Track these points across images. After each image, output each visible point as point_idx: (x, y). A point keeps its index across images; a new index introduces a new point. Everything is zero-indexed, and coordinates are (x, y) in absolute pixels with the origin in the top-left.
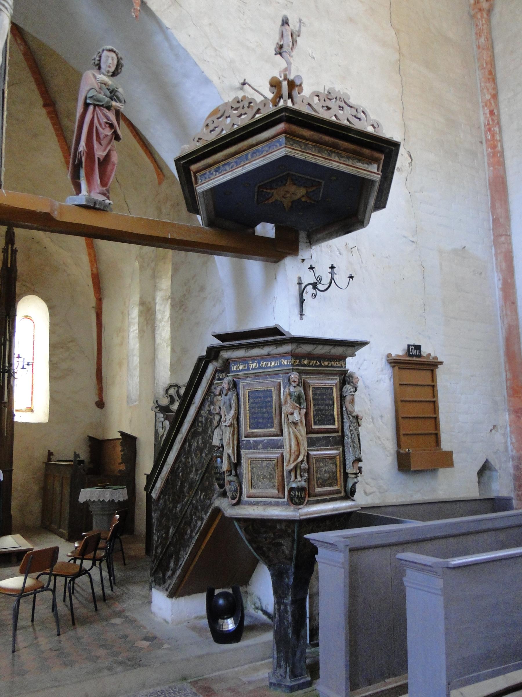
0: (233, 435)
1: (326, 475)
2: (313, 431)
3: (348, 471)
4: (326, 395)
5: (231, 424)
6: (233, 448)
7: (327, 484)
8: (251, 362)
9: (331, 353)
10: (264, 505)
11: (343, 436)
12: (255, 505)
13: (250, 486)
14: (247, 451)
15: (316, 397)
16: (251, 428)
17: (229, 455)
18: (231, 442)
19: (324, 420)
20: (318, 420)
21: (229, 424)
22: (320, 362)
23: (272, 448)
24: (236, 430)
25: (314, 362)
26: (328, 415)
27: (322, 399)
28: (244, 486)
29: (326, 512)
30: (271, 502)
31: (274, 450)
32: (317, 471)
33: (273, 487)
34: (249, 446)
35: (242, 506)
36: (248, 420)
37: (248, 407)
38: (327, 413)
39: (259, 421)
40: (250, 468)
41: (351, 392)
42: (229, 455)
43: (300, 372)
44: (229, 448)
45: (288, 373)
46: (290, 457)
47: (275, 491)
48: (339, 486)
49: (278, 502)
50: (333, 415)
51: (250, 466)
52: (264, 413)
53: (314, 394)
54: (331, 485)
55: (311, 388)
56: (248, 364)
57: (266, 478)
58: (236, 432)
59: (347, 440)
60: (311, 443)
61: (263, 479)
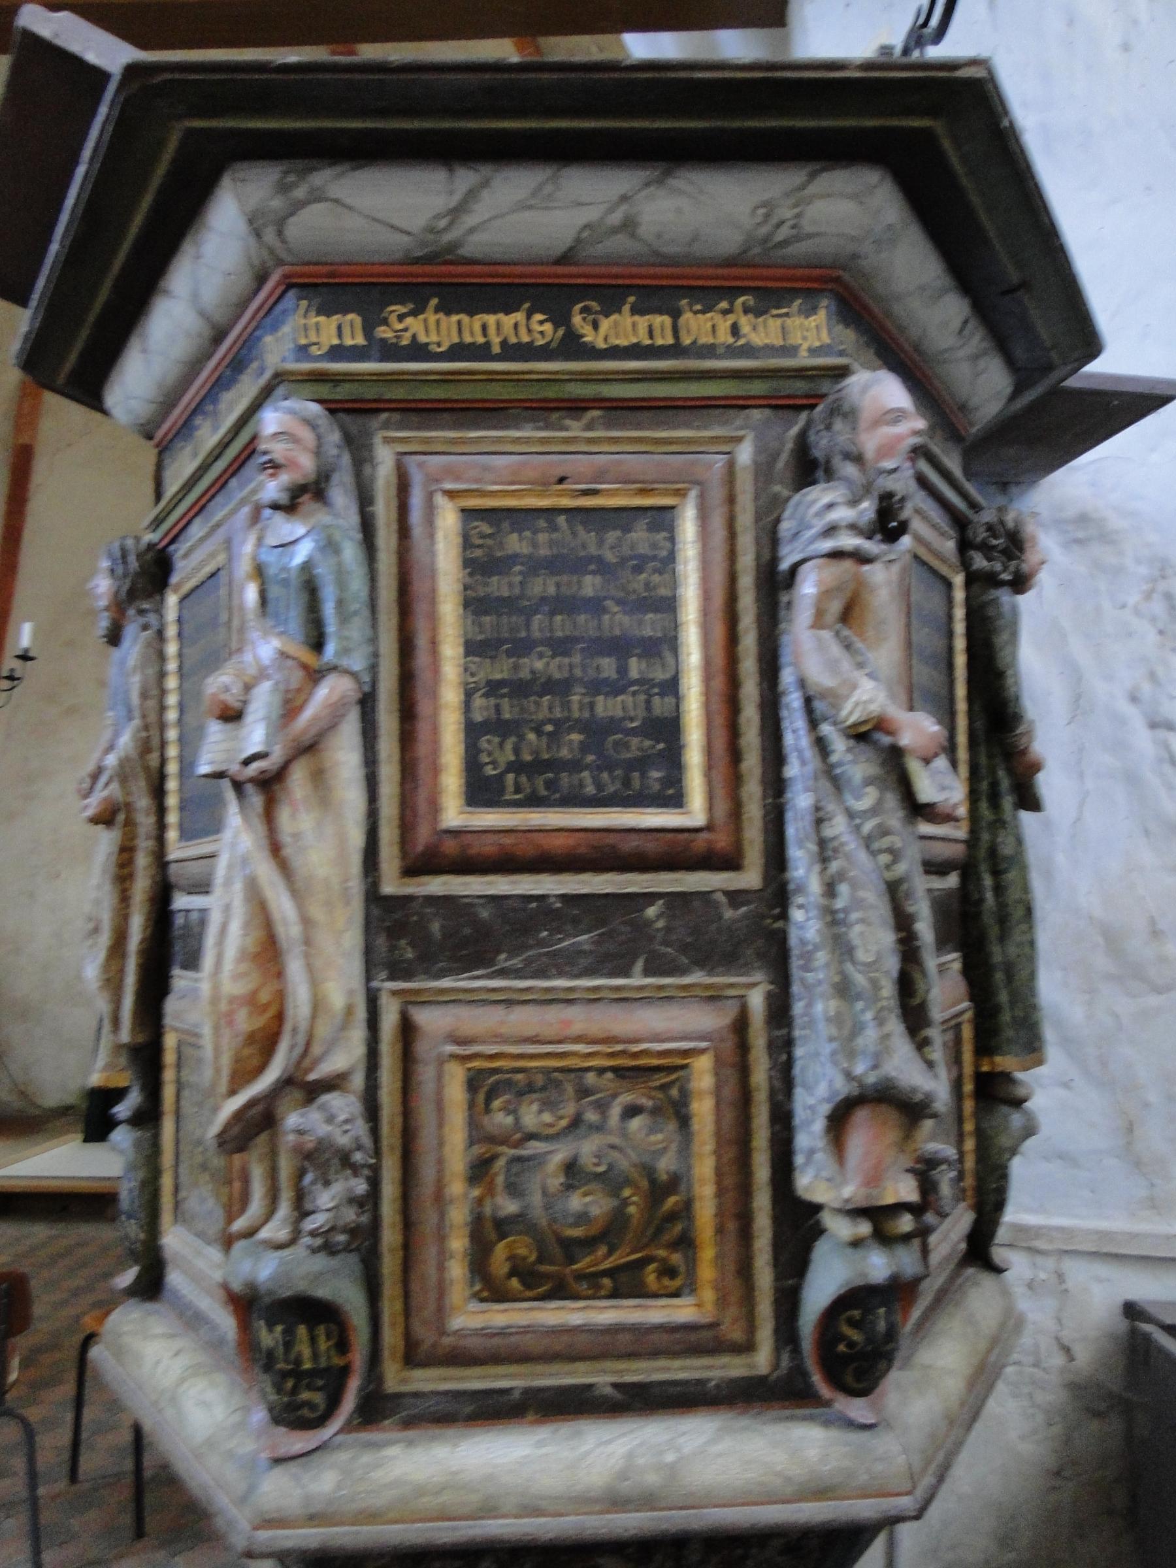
1: (576, 1202)
2: (450, 847)
3: (812, 1182)
4: (603, 568)
7: (593, 1278)
9: (646, 230)
11: (778, 893)
15: (498, 586)
19: (575, 766)
20: (517, 767)
22: (560, 319)
25: (505, 325)
26: (612, 726)
27: (565, 605)
29: (536, 1512)
32: (479, 1171)
38: (606, 707)
41: (831, 530)
43: (353, 410)
48: (708, 1295)
50: (668, 730)
53: (479, 564)
54: (625, 1283)
55: (448, 519)
59: (805, 924)
60: (407, 937)
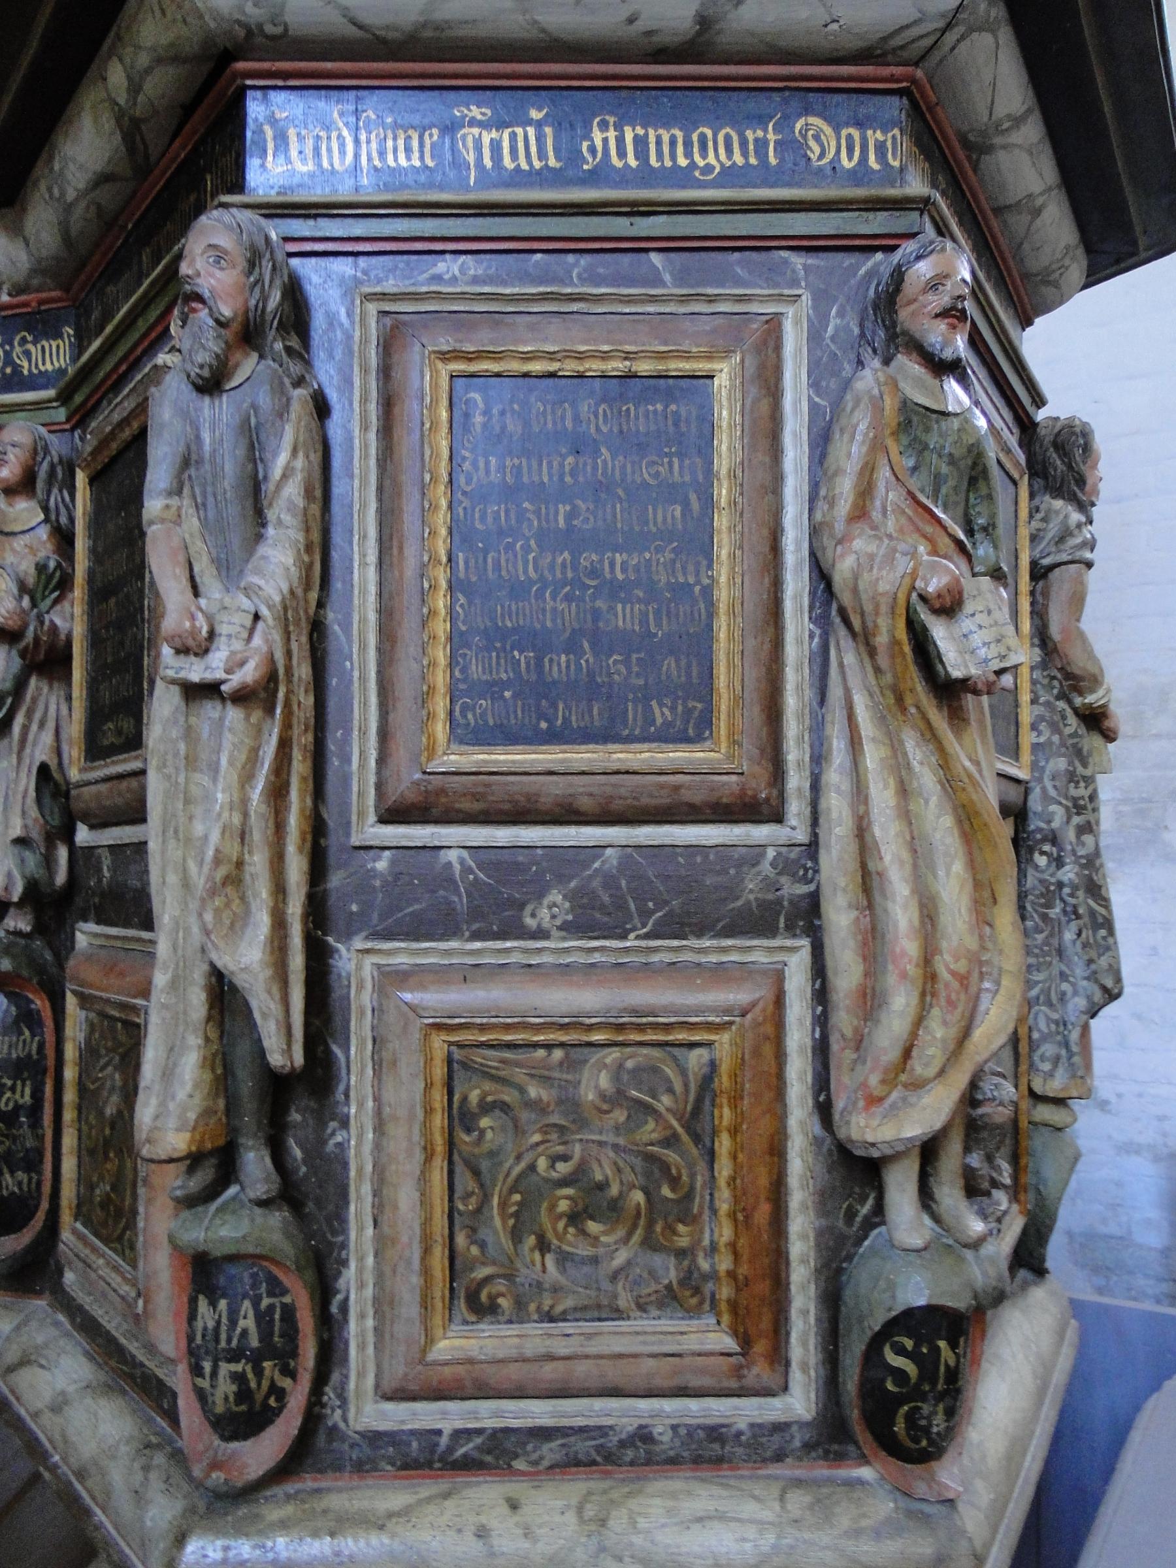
0: (278, 793)
5: (271, 678)
6: (279, 923)
8: (475, 112)
10: (572, 1464)
12: (468, 1465)
13: (440, 1289)
14: (402, 954)
16: (468, 734)
17: (224, 995)
18: (258, 862)
21: (249, 674)
23: (678, 926)
24: (302, 739)
28: (356, 1283)
30: (643, 1436)
31: (707, 949)
33: (686, 1294)
34: (425, 909)
35: (347, 1496)
36: (441, 655)
37: (441, 519)
39: (559, 666)
40: (439, 1120)
42: (224, 995)
44: (238, 924)
45: (886, 244)
46: (919, 1021)
47: (710, 1337)
49: (715, 1433)
51: (439, 1097)
52: (615, 591)
56: (450, 128)
57: (613, 1210)
58: (300, 766)
61: (575, 1218)
